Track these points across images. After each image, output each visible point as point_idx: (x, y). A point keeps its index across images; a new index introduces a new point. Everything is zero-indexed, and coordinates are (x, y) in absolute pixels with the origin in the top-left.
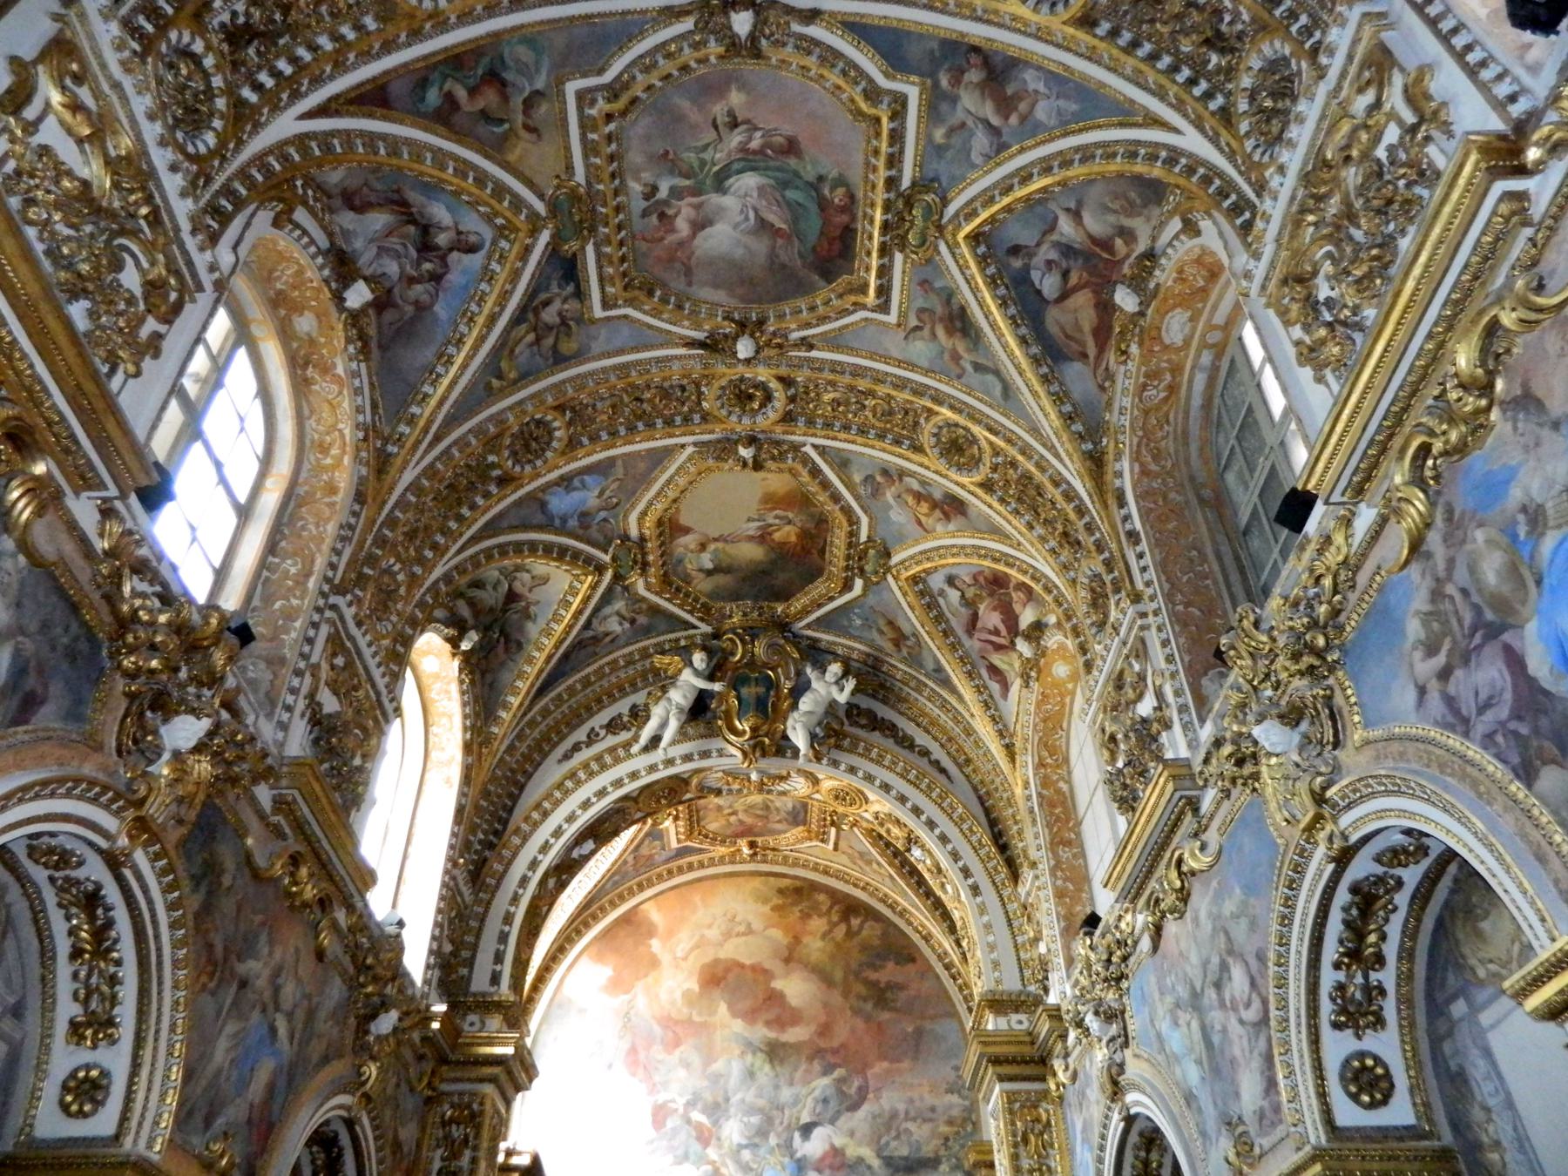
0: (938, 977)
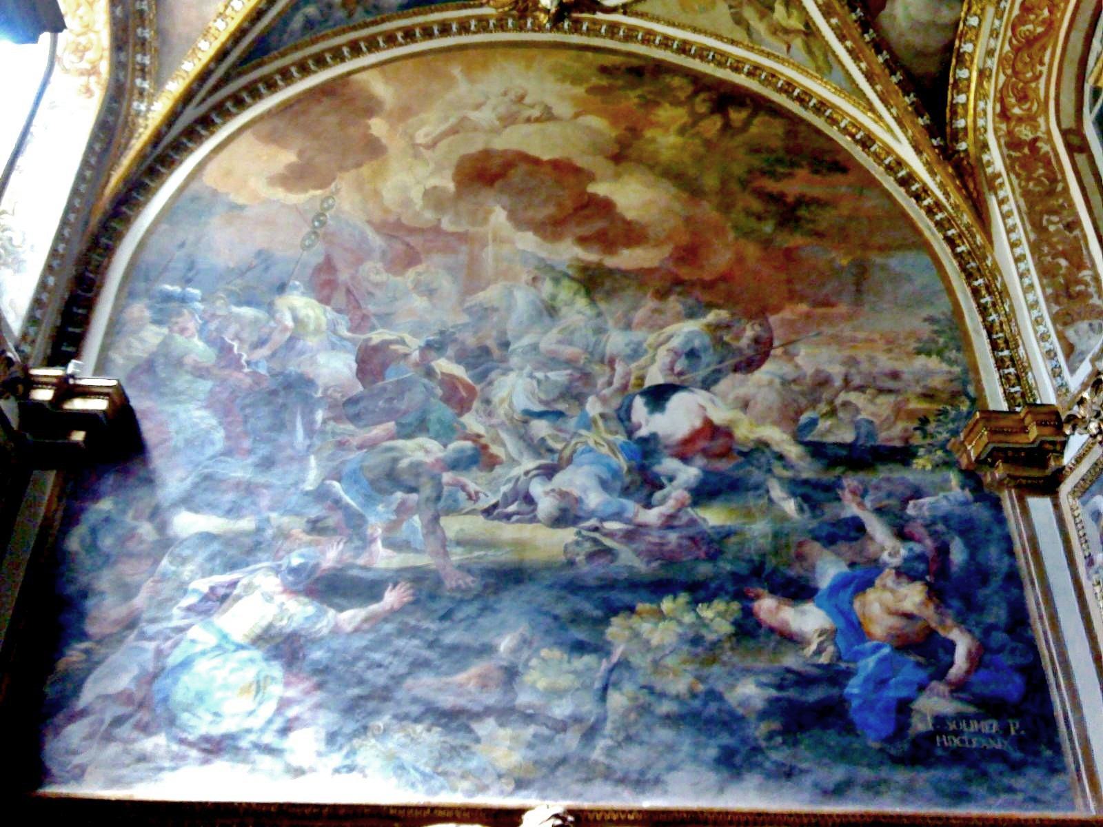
0: (889, 196)
